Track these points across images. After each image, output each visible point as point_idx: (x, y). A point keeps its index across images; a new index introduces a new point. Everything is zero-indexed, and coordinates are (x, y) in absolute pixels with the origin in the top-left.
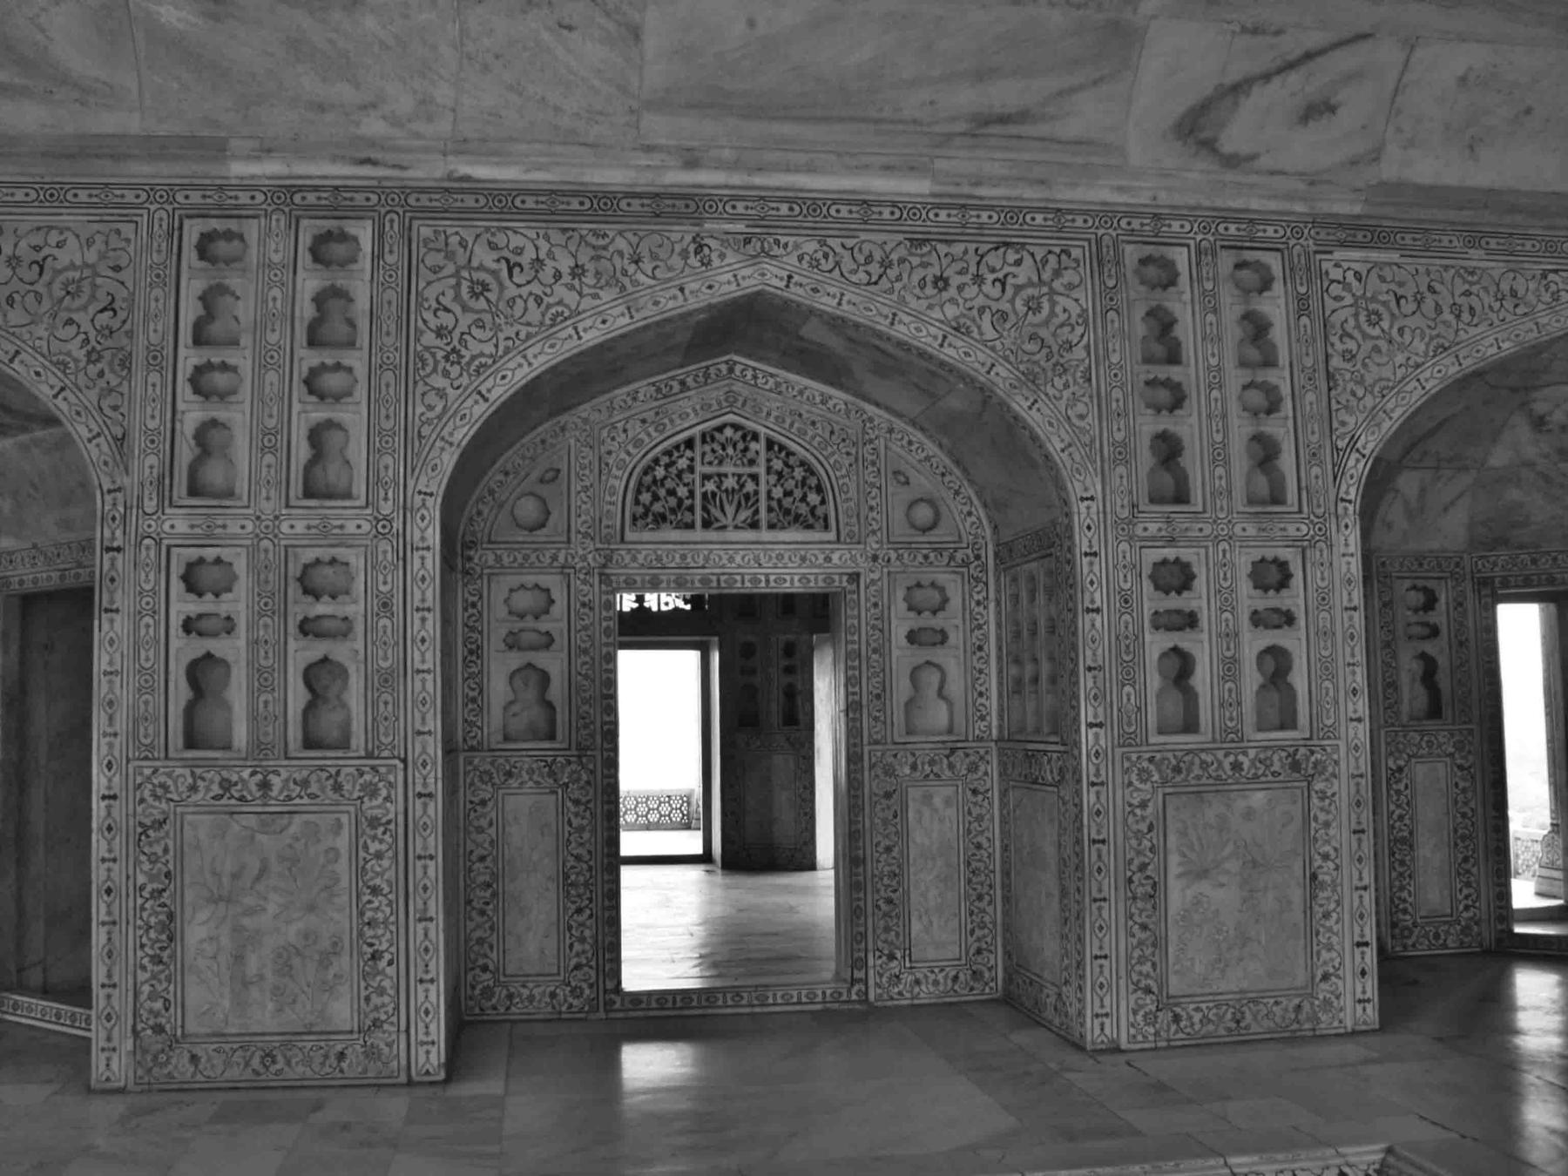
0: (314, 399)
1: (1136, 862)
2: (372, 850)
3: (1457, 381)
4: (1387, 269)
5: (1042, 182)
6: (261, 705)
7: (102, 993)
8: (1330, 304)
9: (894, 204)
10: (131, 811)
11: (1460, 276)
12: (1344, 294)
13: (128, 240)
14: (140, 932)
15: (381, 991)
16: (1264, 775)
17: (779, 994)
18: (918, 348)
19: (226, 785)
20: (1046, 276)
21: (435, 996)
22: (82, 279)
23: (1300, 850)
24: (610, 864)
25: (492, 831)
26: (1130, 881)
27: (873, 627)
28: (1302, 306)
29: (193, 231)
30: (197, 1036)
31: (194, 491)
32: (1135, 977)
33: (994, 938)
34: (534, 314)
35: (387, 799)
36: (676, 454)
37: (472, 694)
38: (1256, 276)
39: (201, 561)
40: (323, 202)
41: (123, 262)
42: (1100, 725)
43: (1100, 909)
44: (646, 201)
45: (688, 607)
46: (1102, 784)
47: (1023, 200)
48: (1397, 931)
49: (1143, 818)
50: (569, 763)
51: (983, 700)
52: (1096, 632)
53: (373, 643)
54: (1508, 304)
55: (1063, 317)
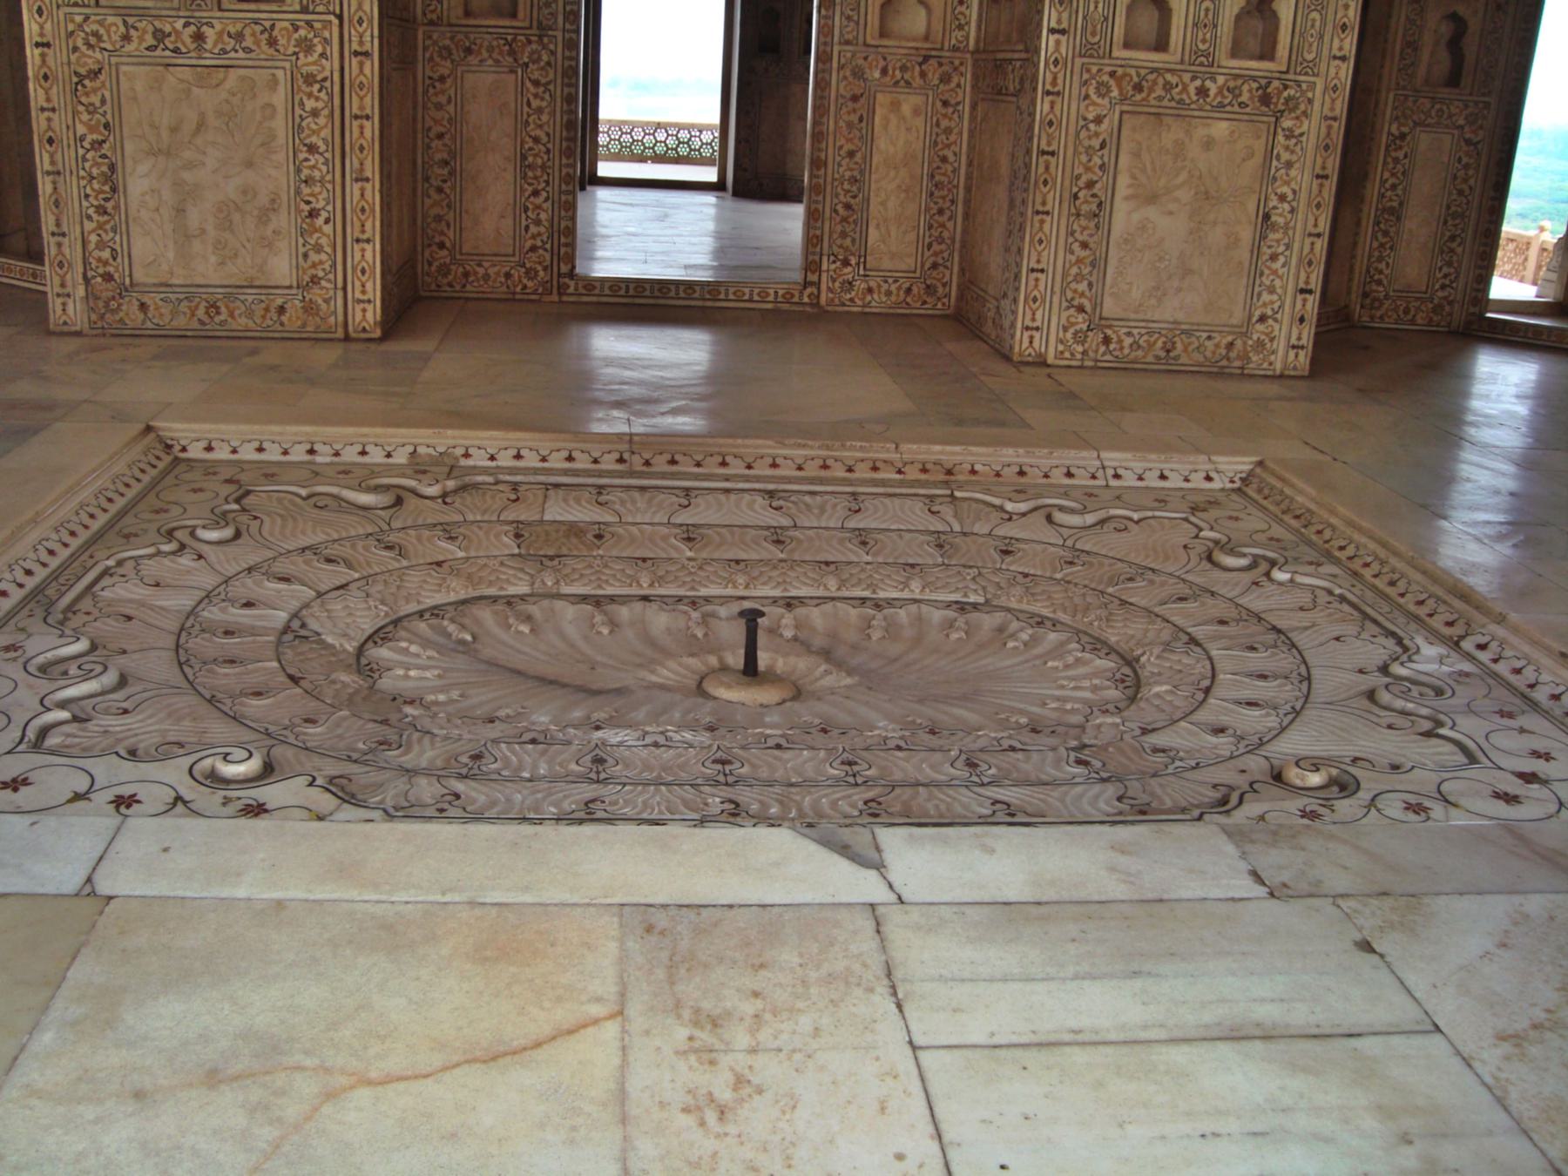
2: (308, 108)
7: (53, 240)
10: (65, 60)
14: (83, 183)
15: (318, 249)
17: (732, 290)
19: (160, 36)
21: (371, 255)
24: (568, 148)
25: (451, 108)
26: (1076, 197)
30: (145, 285)
32: (1069, 295)
35: (323, 55)
42: (1063, 32)
43: (1042, 222)
46: (1058, 93)
48: (1368, 301)
49: (1097, 134)
50: (530, 42)
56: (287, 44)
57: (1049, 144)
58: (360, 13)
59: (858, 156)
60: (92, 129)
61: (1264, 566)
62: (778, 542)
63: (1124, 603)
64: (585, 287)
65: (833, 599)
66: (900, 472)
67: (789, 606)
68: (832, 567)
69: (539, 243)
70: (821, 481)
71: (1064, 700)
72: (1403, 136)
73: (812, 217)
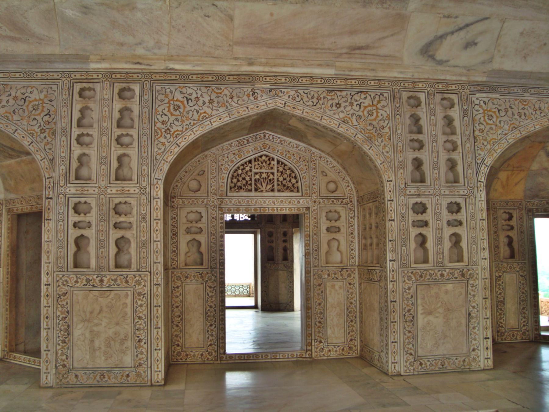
0: (119, 146)
2: (139, 304)
3: (520, 140)
4: (495, 100)
5: (373, 70)
6: (100, 254)
7: (45, 353)
8: (475, 113)
9: (322, 78)
10: (55, 290)
11: (521, 102)
12: (480, 109)
13: (55, 91)
14: (58, 332)
15: (142, 353)
16: (452, 278)
17: (281, 355)
18: (330, 128)
19: (88, 281)
20: (375, 103)
21: (161, 355)
22: (38, 104)
25: (181, 297)
26: (405, 315)
27: (315, 226)
28: (465, 113)
29: (77, 87)
30: (78, 368)
31: (77, 178)
32: (406, 349)
33: (357, 335)
34: (196, 116)
35: (144, 286)
36: (245, 165)
37: (174, 249)
38: (449, 103)
39: (80, 202)
40: (123, 77)
41: (53, 99)
42: (394, 261)
43: (394, 325)
44: (235, 77)
45: (250, 219)
46: (395, 281)
47: (367, 76)
48: (499, 334)
49: (409, 293)
50: (208, 273)
51: (353, 252)
52: (392, 228)
53: (140, 231)
54: (538, 112)
55: (381, 117)
56: (132, 282)
58: (157, 271)
59: (322, 305)
60: (62, 313)
64: (229, 357)
69: (213, 343)
72: (500, 277)
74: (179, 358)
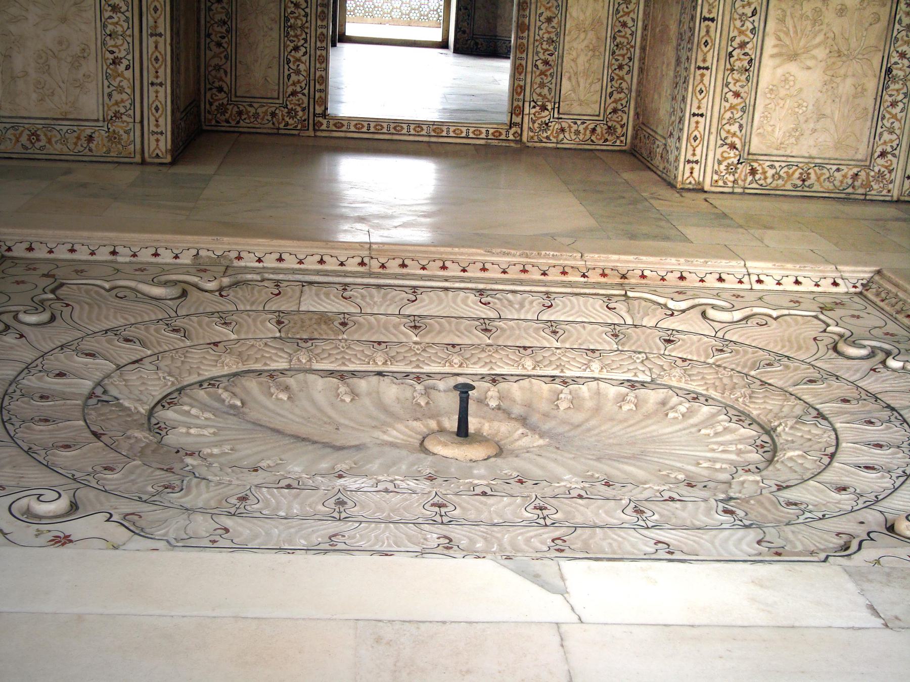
1: (738, 40)
15: (121, 90)
17: (452, 129)
21: (163, 96)
23: (882, 49)
24: (323, 12)
26: (731, 55)
32: (724, 135)
43: (703, 75)
57: (710, 12)
61: (880, 356)
62: (486, 330)
63: (763, 383)
64: (335, 125)
65: (529, 376)
66: (584, 276)
67: (494, 381)
68: (529, 351)
69: (299, 89)
70: (521, 282)
71: (714, 460)
73: (517, 71)
74: (223, 118)
